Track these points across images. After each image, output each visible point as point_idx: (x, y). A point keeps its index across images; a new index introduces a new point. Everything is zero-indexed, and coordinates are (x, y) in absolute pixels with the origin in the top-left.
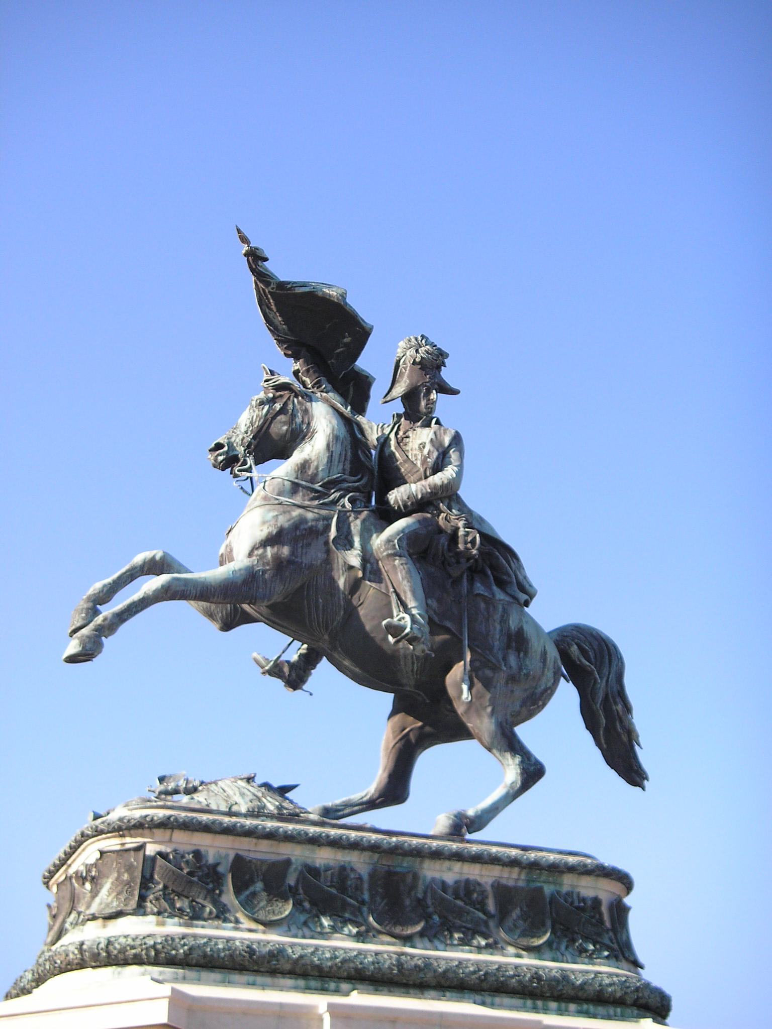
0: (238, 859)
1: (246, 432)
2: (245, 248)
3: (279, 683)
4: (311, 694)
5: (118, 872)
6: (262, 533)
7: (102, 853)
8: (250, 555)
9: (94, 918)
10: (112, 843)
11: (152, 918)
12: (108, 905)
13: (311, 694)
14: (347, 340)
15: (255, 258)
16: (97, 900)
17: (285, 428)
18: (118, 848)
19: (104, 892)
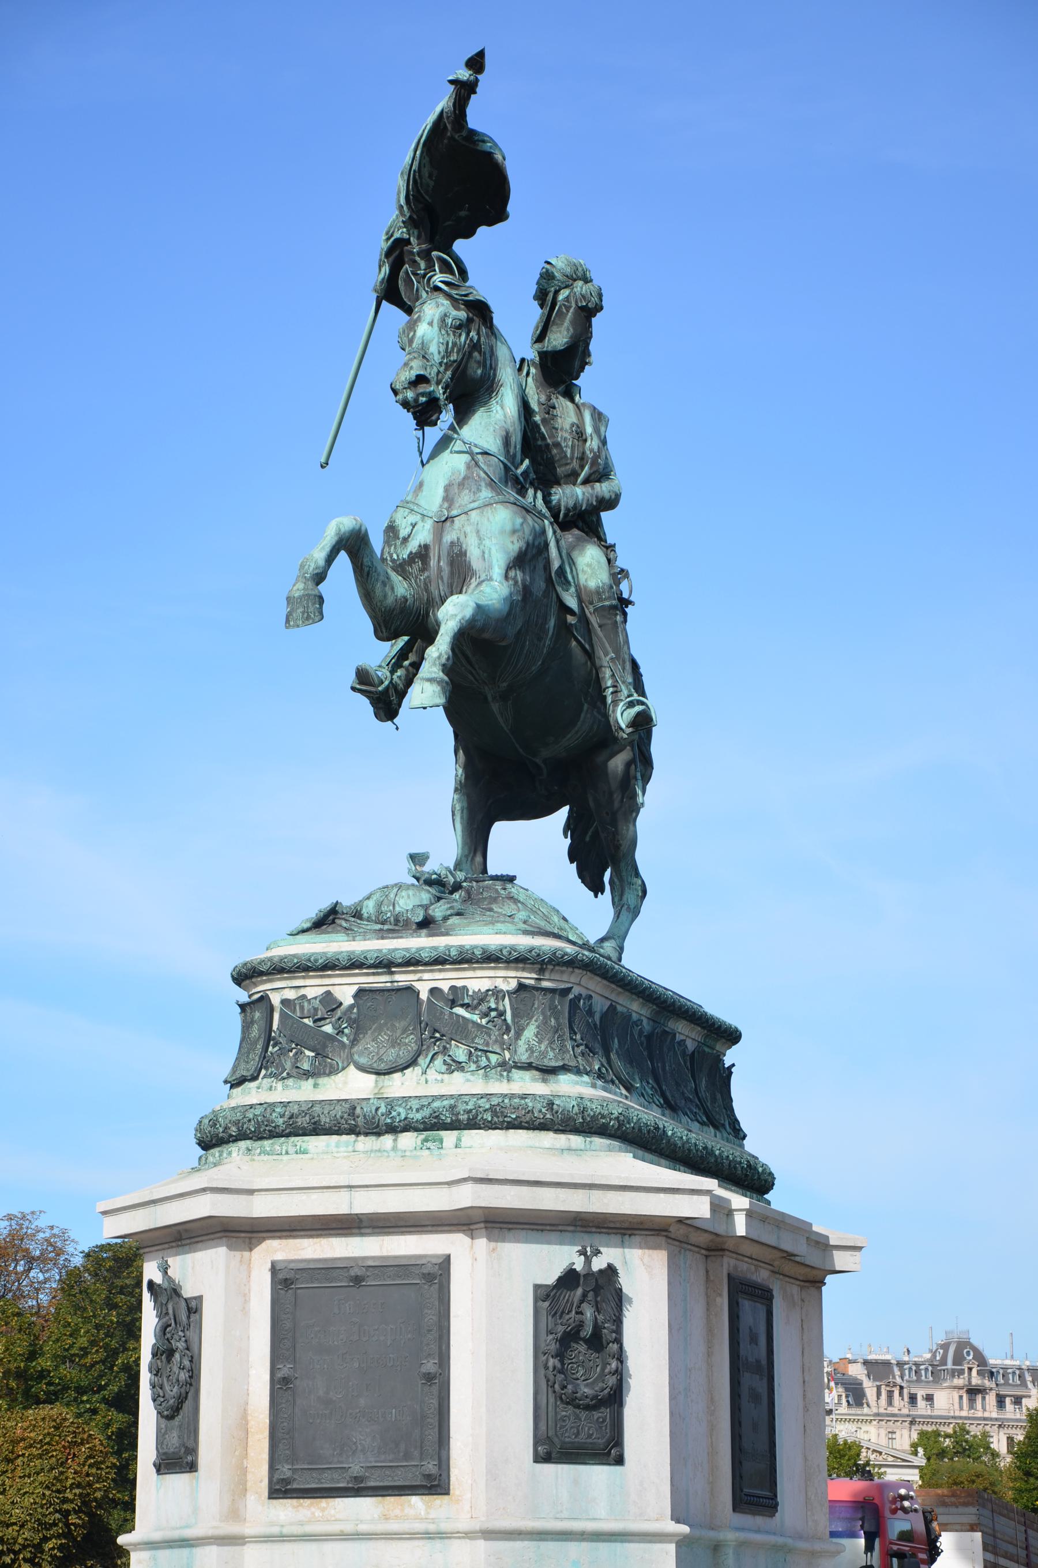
0: (612, 1008)
1: (441, 364)
2: (464, 74)
3: (364, 705)
4: (397, 728)
5: (543, 1013)
6: (515, 546)
7: (521, 987)
8: (506, 577)
9: (529, 1067)
10: (529, 977)
11: (586, 1078)
12: (544, 1054)
13: (397, 728)
14: (463, 213)
15: (464, 91)
16: (522, 1045)
17: (479, 372)
18: (532, 982)
19: (530, 1032)
